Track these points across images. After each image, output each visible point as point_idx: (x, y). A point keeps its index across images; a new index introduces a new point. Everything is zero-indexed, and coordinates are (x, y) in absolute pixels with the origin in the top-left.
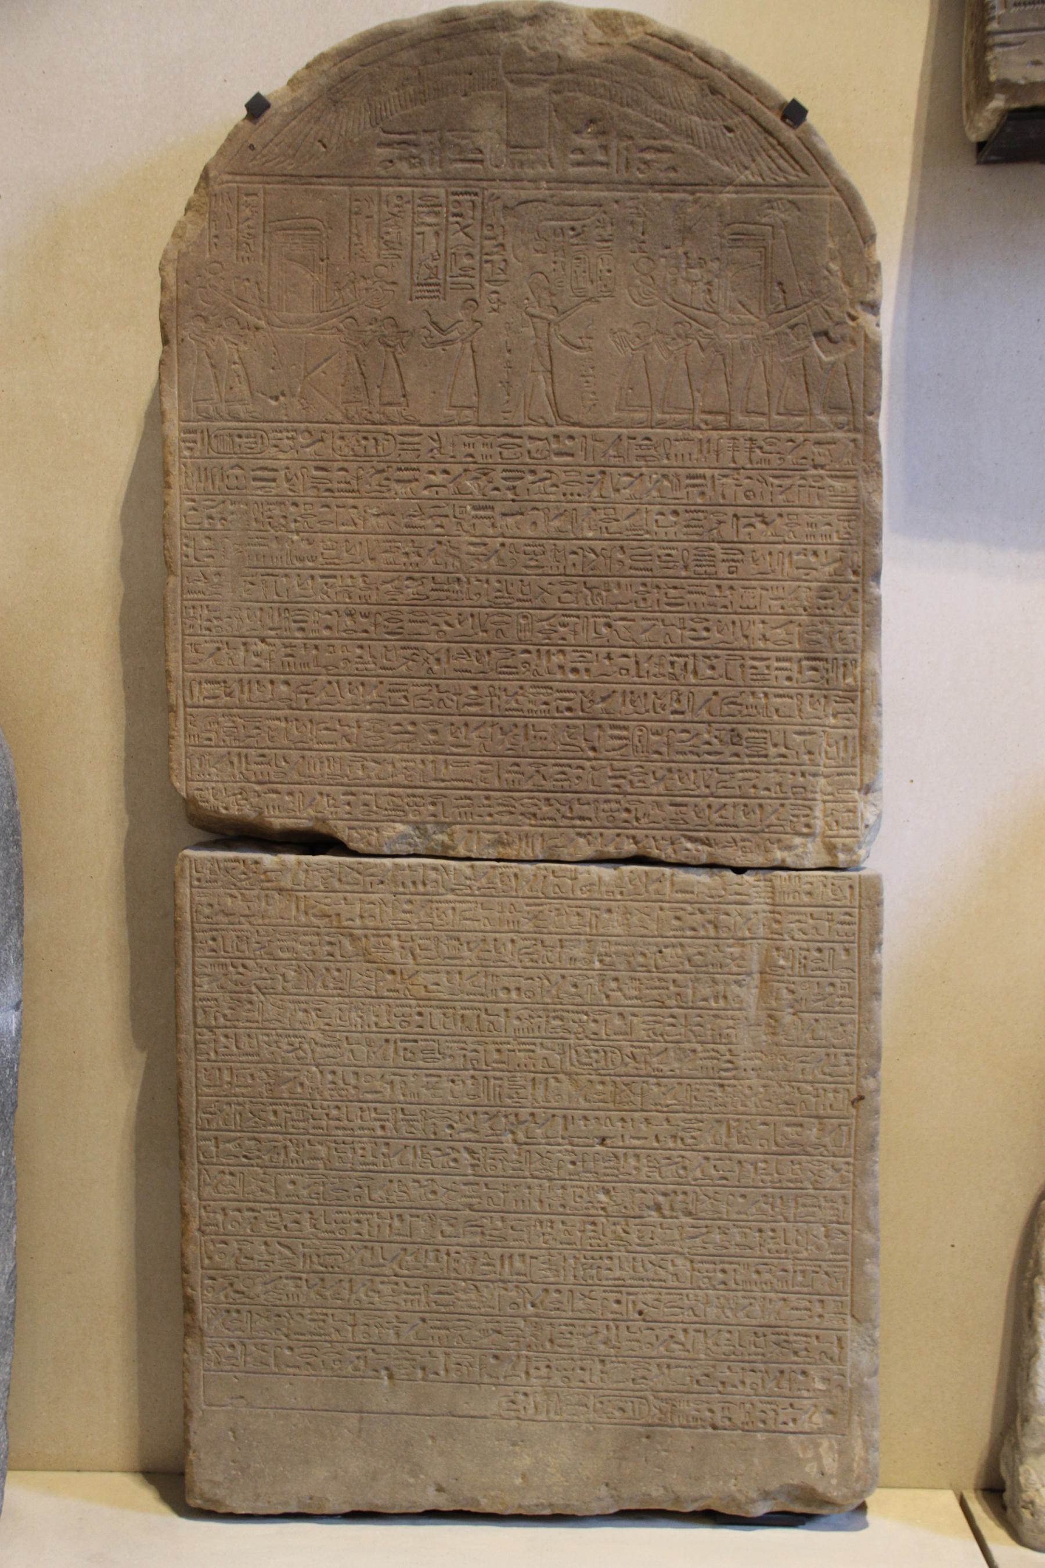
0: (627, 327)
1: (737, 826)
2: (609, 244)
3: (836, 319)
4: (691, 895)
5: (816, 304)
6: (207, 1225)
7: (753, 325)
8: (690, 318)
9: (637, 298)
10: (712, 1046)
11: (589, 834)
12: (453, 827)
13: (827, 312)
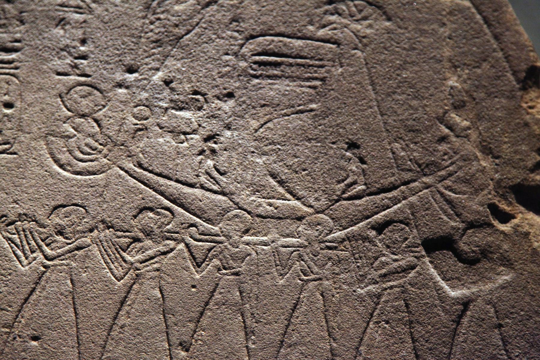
0: (41, 214)
2: (14, 56)
3: (471, 217)
5: (427, 186)
7: (300, 219)
8: (174, 201)
9: (64, 157)
13: (449, 202)
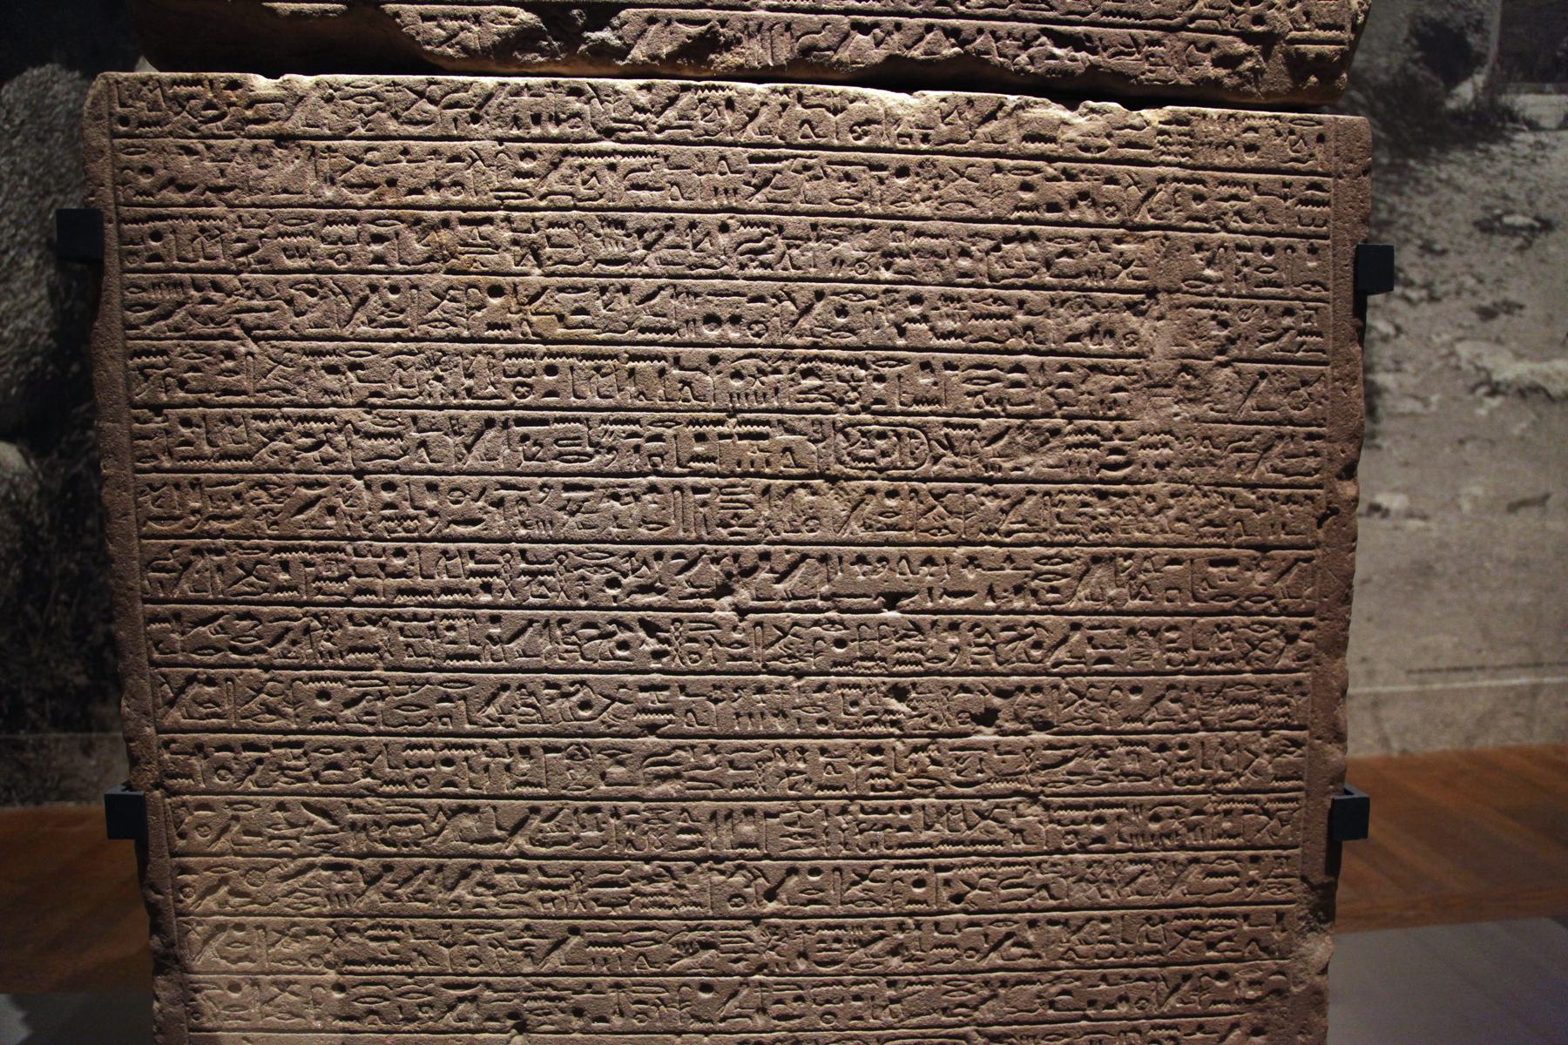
1: (1137, 16)
4: (1052, 146)
6: (174, 776)
10: (1089, 422)
11: (876, 25)
12: (623, 14)
